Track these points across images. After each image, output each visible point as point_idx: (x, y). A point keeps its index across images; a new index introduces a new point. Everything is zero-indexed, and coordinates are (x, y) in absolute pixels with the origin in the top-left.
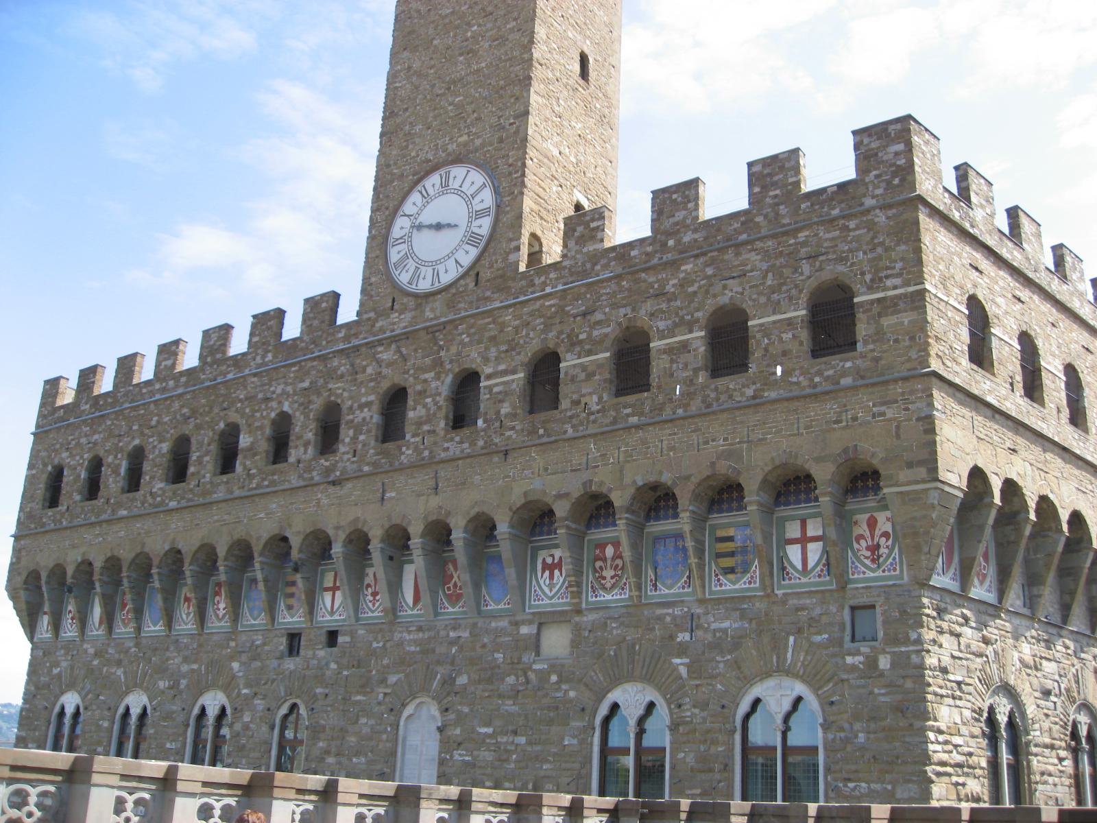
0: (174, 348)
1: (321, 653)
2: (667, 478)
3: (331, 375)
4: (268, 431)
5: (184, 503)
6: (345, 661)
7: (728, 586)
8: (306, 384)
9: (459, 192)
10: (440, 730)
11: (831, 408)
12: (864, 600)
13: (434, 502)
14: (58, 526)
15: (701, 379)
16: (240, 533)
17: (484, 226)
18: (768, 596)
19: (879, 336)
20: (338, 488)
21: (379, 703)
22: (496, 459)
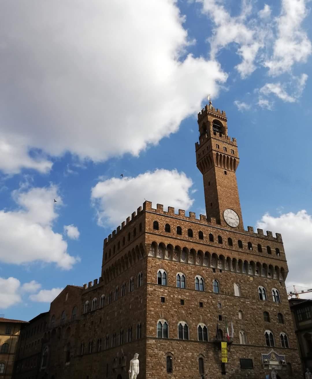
0: (184, 211)
1: (220, 273)
2: (266, 263)
3: (219, 232)
4: (209, 235)
5: (194, 241)
6: (224, 275)
7: (268, 277)
8: (215, 231)
9: (233, 214)
10: (240, 288)
11: (279, 261)
12: (281, 281)
13: (239, 257)
14: (160, 234)
15: (267, 253)
16: (207, 250)
17: (238, 221)
18: (273, 279)
19: (282, 256)
20: (224, 250)
21: (231, 282)
22: (247, 254)
